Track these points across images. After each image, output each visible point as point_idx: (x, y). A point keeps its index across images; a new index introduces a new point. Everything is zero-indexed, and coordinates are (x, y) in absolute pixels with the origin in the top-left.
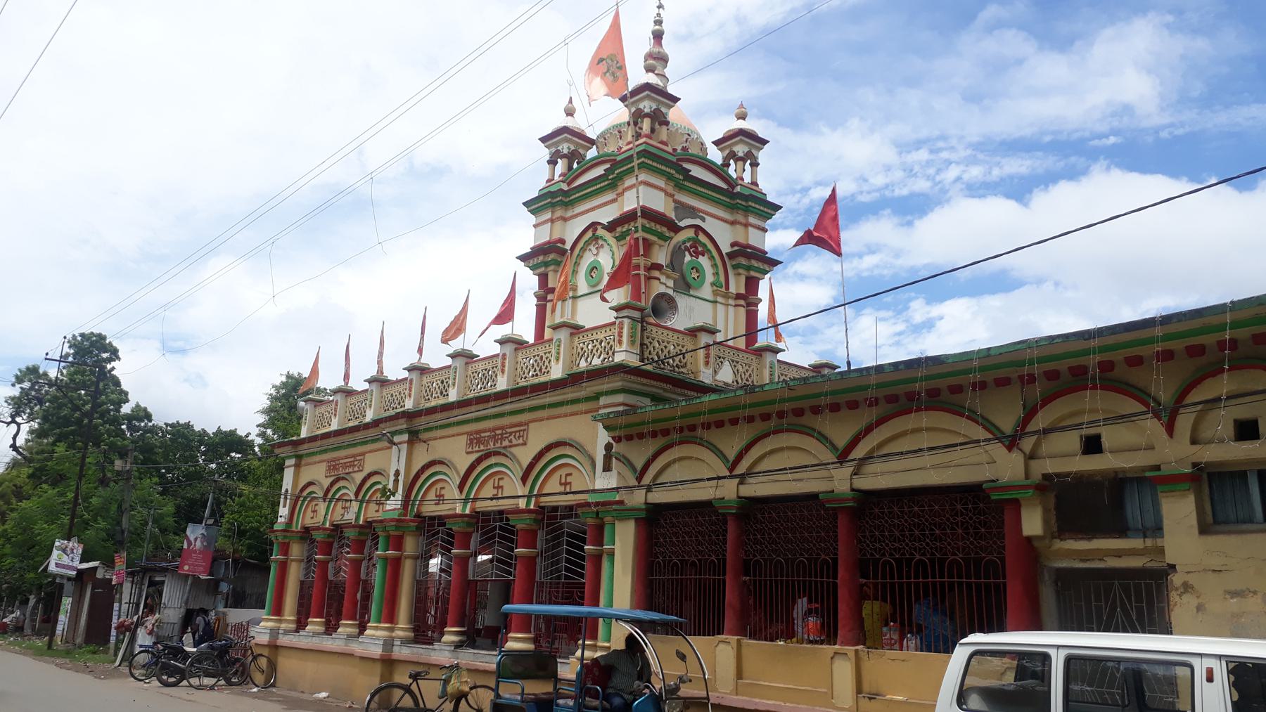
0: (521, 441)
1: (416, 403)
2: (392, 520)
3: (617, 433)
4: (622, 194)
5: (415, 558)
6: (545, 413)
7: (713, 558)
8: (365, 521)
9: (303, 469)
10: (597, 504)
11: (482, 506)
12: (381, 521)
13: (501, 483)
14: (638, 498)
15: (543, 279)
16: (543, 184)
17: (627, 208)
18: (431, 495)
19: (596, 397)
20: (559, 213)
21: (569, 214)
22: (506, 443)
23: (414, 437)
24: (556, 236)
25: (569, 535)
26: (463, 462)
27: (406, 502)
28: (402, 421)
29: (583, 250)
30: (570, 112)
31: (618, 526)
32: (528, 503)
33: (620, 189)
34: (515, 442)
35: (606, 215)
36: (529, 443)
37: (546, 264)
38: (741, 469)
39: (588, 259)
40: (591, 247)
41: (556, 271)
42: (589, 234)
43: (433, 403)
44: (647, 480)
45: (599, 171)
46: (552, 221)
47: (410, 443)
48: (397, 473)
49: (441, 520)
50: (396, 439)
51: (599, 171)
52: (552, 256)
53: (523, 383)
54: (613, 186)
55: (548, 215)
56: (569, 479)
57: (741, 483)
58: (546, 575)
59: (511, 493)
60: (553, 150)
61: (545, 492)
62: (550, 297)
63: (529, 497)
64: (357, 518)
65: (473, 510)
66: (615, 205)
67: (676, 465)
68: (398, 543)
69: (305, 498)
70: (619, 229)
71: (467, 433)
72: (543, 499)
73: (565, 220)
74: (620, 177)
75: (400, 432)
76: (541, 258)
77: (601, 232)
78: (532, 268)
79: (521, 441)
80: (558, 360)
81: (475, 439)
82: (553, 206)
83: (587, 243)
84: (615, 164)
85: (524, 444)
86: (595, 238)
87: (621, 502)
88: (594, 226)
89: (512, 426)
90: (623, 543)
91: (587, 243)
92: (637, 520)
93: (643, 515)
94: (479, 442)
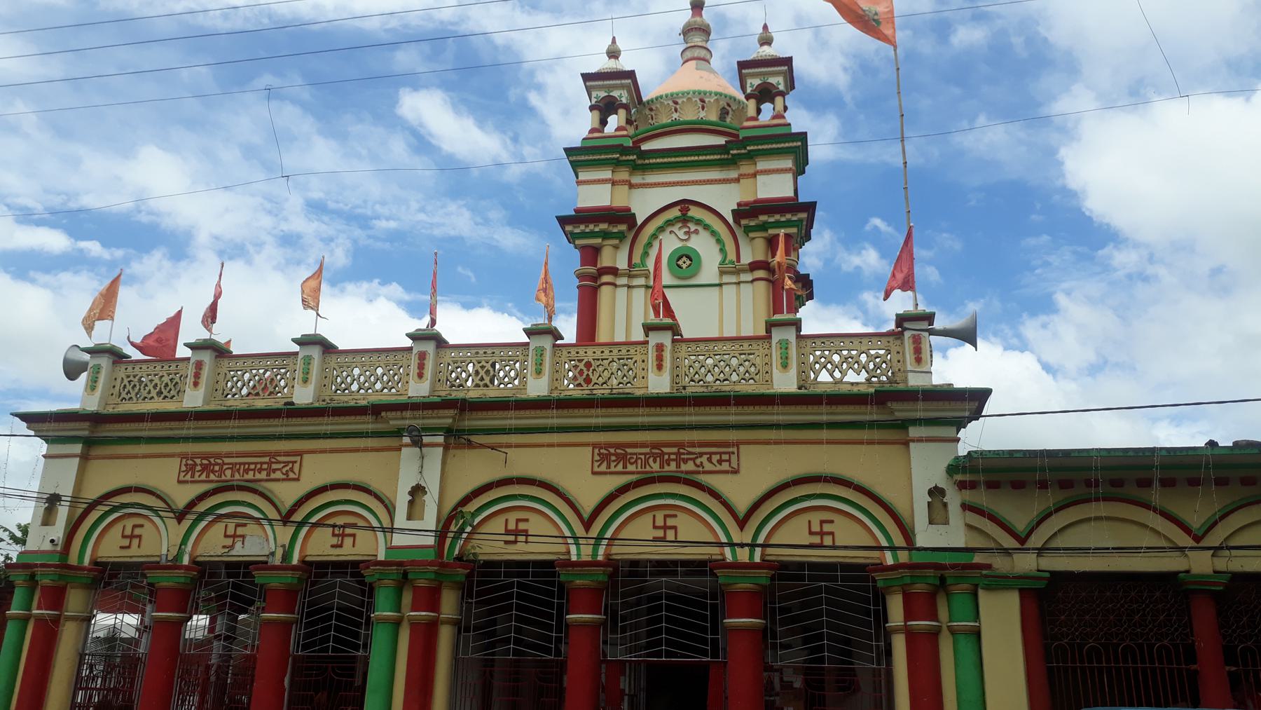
0: (725, 466)
1: (433, 385)
2: (431, 563)
3: (959, 477)
4: (754, 175)
5: (456, 623)
6: (825, 434)
7: (1165, 642)
8: (303, 561)
9: (94, 465)
10: (954, 566)
11: (623, 551)
12: (400, 564)
13: (670, 522)
14: (1026, 563)
15: (589, 255)
16: (585, 134)
17: (762, 195)
18: (497, 525)
19: (904, 425)
20: (623, 175)
21: (636, 179)
22: (690, 466)
23: (456, 438)
24: (619, 203)
25: (669, 597)
26: (589, 488)
27: (441, 534)
28: (452, 412)
29: (661, 229)
30: (613, 54)
31: (983, 596)
32: (752, 555)
33: (746, 168)
34: (708, 467)
35: (723, 197)
36: (742, 470)
37: (606, 235)
38: (1214, 539)
39: (670, 244)
40: (675, 229)
41: (616, 247)
42: (675, 212)
43: (474, 394)
44: (1036, 541)
45: (721, 141)
46: (614, 183)
47: (446, 447)
48: (417, 491)
49: (520, 567)
50: (426, 440)
51: (721, 141)
52: (623, 227)
53: (726, 388)
54: (732, 162)
55: (607, 174)
56: (827, 528)
57: (1213, 556)
58: (305, 647)
59: (693, 534)
60: (603, 94)
61: (772, 542)
62: (606, 278)
63: (753, 546)
64: (287, 555)
65: (607, 555)
66: (733, 187)
67: (1085, 527)
68: (430, 599)
69: (115, 509)
70: (763, 218)
71: (594, 446)
72: (769, 551)
73: (631, 186)
74: (751, 157)
75: (432, 430)
76: (603, 226)
77: (694, 212)
78: (571, 238)
79: (725, 466)
80: (785, 366)
81: (607, 456)
82: (616, 164)
83: (669, 223)
84: (735, 140)
85: (736, 472)
86: (684, 220)
87: (989, 567)
88: (685, 204)
89: (702, 444)
90: (1001, 620)
91: (669, 223)
92: (1023, 593)
93: (1041, 585)
94: (623, 458)
